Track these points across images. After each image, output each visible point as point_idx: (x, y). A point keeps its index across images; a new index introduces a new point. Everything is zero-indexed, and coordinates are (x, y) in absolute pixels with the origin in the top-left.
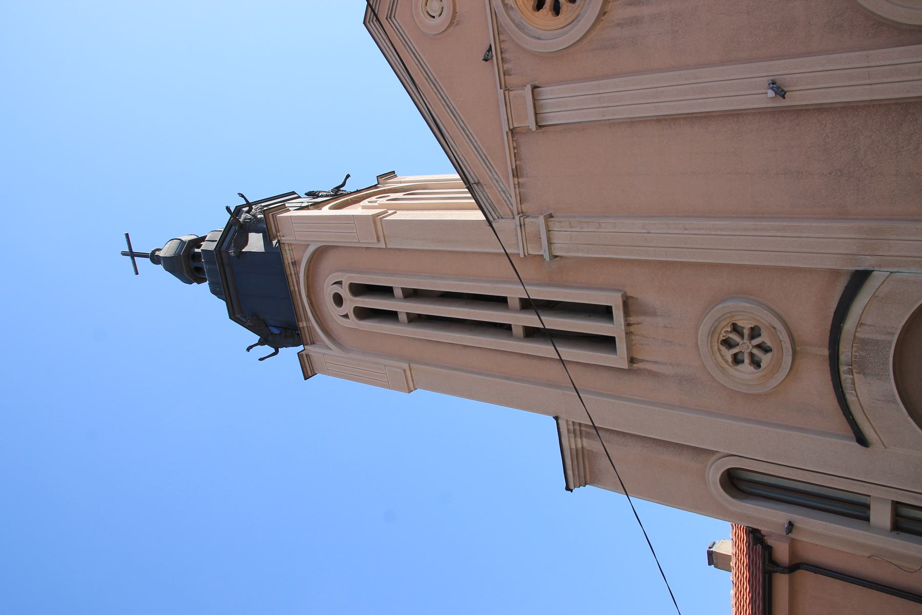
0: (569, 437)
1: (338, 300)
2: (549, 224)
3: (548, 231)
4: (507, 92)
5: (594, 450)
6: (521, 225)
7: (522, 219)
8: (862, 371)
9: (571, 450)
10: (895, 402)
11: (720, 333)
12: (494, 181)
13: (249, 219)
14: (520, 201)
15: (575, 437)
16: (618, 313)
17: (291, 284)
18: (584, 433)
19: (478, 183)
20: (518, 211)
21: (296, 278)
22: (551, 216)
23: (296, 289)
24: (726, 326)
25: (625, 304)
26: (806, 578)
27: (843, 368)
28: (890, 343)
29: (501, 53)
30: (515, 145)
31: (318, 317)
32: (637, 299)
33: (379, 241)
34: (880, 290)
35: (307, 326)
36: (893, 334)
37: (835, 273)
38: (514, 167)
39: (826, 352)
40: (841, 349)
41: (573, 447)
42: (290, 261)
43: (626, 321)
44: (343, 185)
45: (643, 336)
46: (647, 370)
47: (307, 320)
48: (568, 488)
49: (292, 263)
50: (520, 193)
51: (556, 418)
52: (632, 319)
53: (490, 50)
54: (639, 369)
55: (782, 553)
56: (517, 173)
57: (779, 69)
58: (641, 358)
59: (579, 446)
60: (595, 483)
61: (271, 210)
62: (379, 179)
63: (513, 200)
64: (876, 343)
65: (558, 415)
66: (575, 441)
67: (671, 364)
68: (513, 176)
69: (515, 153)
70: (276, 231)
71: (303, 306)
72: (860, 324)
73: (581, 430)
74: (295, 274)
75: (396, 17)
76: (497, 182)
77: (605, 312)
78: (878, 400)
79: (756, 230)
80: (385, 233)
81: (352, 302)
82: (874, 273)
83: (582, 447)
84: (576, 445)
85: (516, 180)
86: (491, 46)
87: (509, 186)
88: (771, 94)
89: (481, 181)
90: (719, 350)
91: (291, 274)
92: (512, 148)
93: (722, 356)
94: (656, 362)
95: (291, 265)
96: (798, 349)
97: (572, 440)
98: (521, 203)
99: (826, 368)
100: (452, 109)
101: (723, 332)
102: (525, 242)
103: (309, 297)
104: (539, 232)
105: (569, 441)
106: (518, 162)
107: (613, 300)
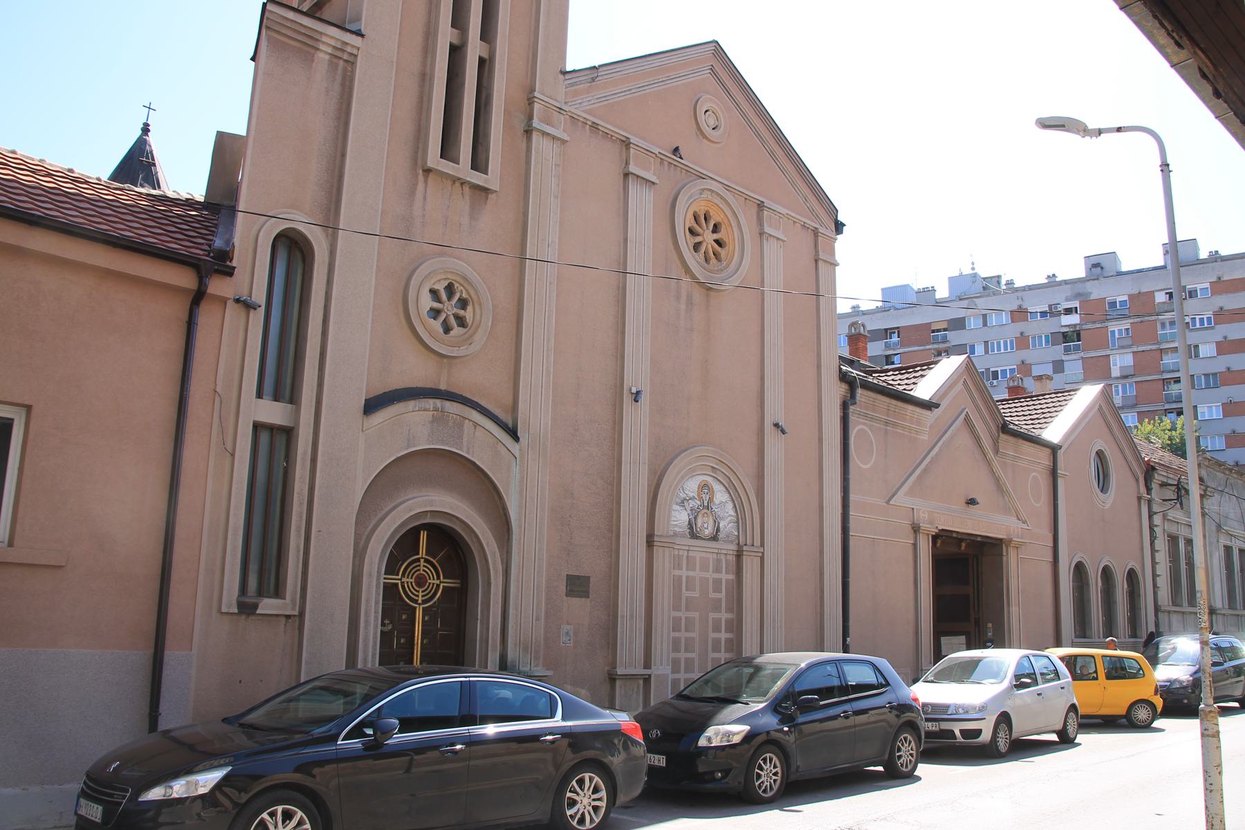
0: (338, 40)
2: (559, 142)
5: (314, 64)
6: (560, 109)
8: (435, 420)
9: (321, 33)
10: (408, 446)
11: (461, 285)
12: (590, 99)
14: (573, 117)
15: (334, 48)
18: (335, 60)
24: (468, 293)
25: (485, 190)
27: (438, 403)
28: (463, 451)
29: (675, 165)
30: (614, 138)
32: (486, 203)
34: (503, 446)
36: (468, 453)
38: (600, 128)
39: (443, 387)
40: (455, 404)
43: (469, 183)
45: (451, 195)
46: (417, 184)
52: (466, 189)
53: (681, 158)
54: (417, 175)
56: (594, 126)
57: (644, 398)
58: (429, 182)
59: (322, 47)
60: (268, 42)
64: (460, 437)
66: (329, 45)
67: (424, 216)
68: (594, 123)
69: (608, 134)
72: (476, 424)
73: (341, 58)
77: (479, 163)
78: (409, 430)
79: (548, 350)
83: (318, 49)
84: (324, 43)
85: (590, 123)
86: (682, 159)
88: (634, 390)
90: (445, 279)
92: (612, 133)
94: (425, 198)
96: (445, 360)
97: (332, 42)
99: (429, 385)
101: (462, 288)
104: (553, 127)
105: (332, 37)
106: (601, 133)
107: (491, 179)
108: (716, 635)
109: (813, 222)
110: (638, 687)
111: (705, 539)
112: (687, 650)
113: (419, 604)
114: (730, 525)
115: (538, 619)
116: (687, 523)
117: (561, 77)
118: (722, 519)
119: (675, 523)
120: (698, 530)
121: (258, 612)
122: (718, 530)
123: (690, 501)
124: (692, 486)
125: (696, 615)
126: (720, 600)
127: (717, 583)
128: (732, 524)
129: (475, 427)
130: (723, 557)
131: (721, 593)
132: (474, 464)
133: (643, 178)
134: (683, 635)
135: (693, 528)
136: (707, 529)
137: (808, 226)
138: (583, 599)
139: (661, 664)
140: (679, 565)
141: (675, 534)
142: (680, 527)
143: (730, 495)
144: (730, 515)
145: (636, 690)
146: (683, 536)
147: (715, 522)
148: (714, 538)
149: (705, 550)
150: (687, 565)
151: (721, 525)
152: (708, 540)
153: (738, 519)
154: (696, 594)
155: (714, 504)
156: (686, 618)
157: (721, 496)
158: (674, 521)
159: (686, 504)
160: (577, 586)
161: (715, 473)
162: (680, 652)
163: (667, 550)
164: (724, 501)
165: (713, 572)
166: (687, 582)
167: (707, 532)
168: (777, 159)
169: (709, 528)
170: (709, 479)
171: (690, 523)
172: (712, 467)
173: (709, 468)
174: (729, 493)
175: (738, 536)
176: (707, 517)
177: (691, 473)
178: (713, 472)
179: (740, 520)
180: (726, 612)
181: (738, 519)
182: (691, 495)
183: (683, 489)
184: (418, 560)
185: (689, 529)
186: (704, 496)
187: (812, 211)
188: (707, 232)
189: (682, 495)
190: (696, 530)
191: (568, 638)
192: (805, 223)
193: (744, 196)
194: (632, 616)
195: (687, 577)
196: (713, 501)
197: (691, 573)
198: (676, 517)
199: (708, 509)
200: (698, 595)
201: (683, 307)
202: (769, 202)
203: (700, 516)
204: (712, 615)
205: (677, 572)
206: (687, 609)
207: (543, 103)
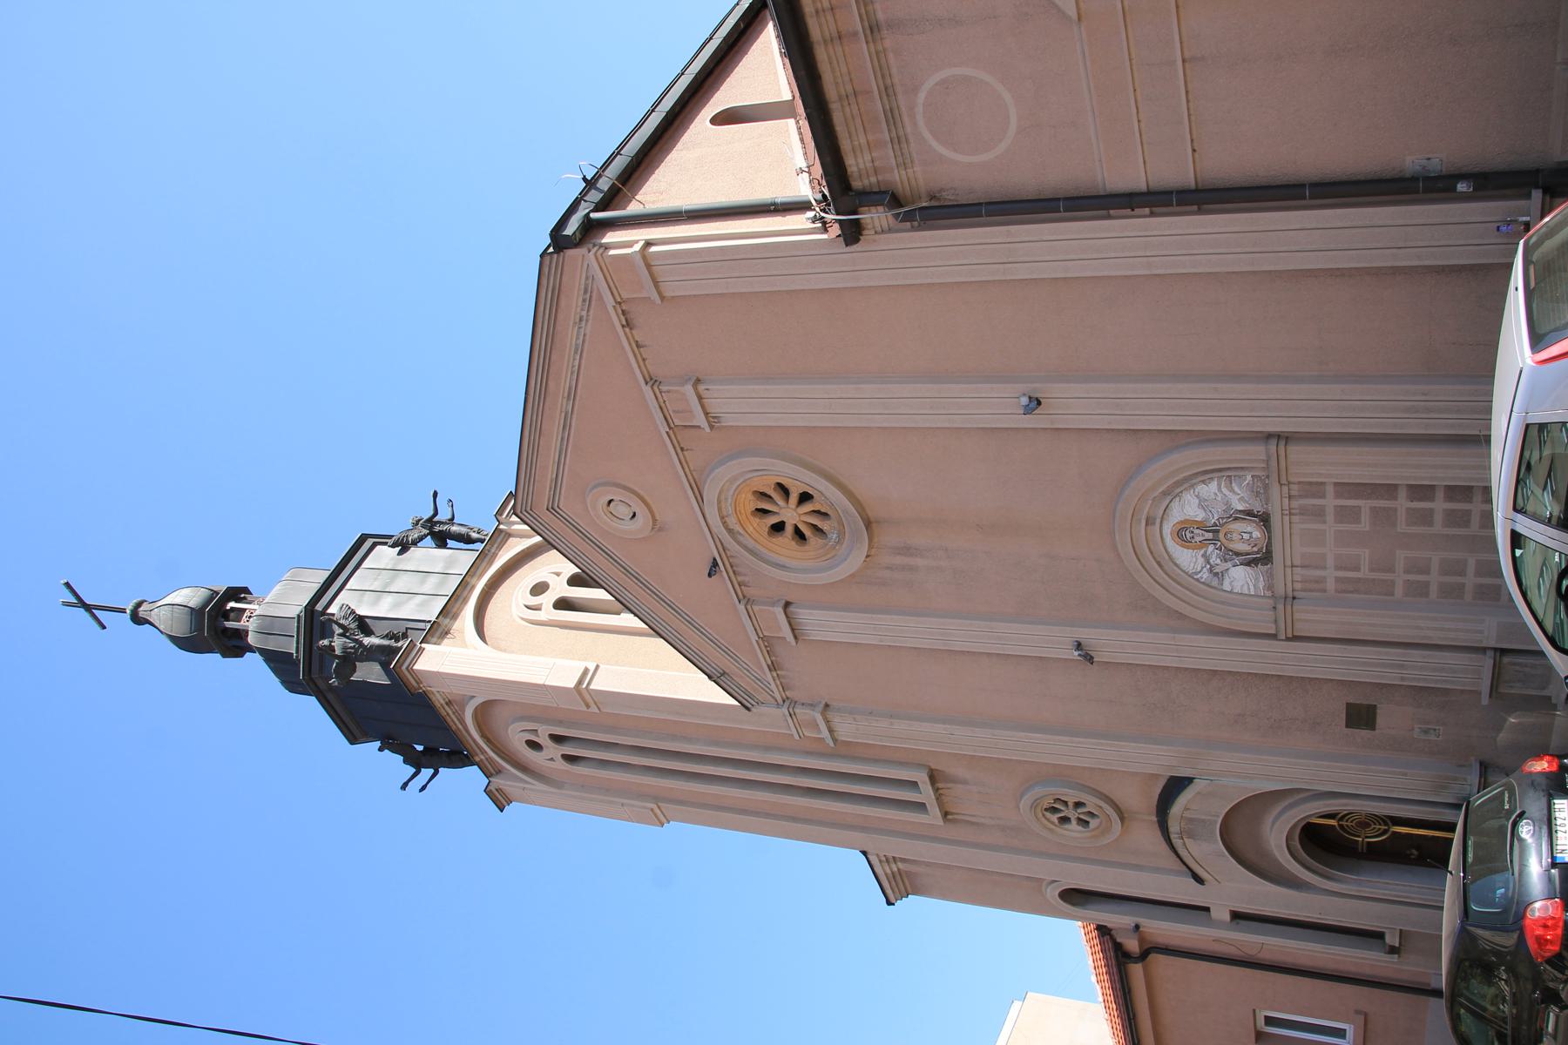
1: (534, 745)
3: (700, 398)
4: (749, 607)
6: (790, 715)
7: (655, 388)
9: (886, 874)
12: (745, 671)
13: (351, 648)
16: (926, 794)
17: (451, 724)
19: (724, 673)
20: (782, 698)
21: (456, 716)
22: (698, 381)
23: (460, 727)
26: (1159, 961)
28: (1216, 822)
29: (732, 566)
31: (504, 753)
32: (942, 771)
33: (588, 706)
35: (487, 759)
36: (1218, 816)
37: (1156, 776)
38: (770, 663)
41: (889, 871)
42: (442, 702)
44: (436, 513)
47: (483, 752)
48: (889, 903)
49: (447, 704)
50: (781, 683)
51: (864, 853)
55: (1132, 945)
56: (773, 667)
59: (895, 869)
61: (401, 661)
62: (499, 518)
63: (773, 686)
65: (865, 849)
68: (770, 670)
69: (768, 651)
70: (418, 683)
71: (474, 741)
74: (454, 713)
75: (561, 507)
76: (748, 671)
80: (596, 700)
81: (553, 751)
82: (1195, 780)
86: (715, 559)
87: (764, 673)
89: (727, 671)
90: (1044, 815)
91: (448, 714)
92: (763, 648)
93: (1048, 820)
95: (445, 706)
98: (784, 691)
100: (669, 603)
102: (797, 725)
103: (483, 736)
108: (1438, 518)
109: (600, 297)
110: (1514, 664)
111: (1270, 538)
112: (1462, 573)
113: (1389, 828)
114: (1236, 489)
115: (1405, 774)
116: (1245, 567)
117: (753, 709)
118: (1228, 504)
119: (1252, 588)
120: (1255, 549)
121: (1397, 945)
122: (1249, 513)
124: (1188, 559)
125: (1401, 556)
126: (1374, 510)
127: (1344, 514)
128: (1233, 485)
129: (1188, 809)
130: (1295, 504)
131: (1360, 507)
132: (1227, 812)
133: (790, 624)
134: (1434, 579)
135: (1254, 559)
137: (623, 318)
138: (1378, 711)
139: (1481, 632)
140: (1317, 582)
141: (1270, 587)
142: (1257, 579)
144: (1219, 489)
145: (1517, 668)
146: (1270, 576)
147: (1236, 519)
148: (1264, 520)
150: (1317, 568)
152: (1269, 532)
154: (1365, 554)
156: (1407, 571)
157: (1188, 508)
158: (1249, 589)
159: (1217, 570)
160: (1361, 716)
161: (1155, 519)
162: (1463, 585)
163: (1297, 616)
164: (1197, 501)
165: (1325, 522)
166: (1346, 569)
167: (1257, 534)
168: (570, 388)
169: (1249, 529)
170: (1168, 529)
171: (1248, 564)
172: (1147, 525)
173: (1149, 528)
176: (1231, 533)
177: (1165, 563)
178: (1154, 524)
179: (1226, 473)
180: (1395, 498)
182: (1201, 561)
183: (1197, 573)
184: (1339, 825)
187: (588, 302)
188: (783, 511)
189: (1205, 575)
190: (1257, 553)
191: (1432, 731)
192: (623, 326)
193: (682, 457)
194: (1401, 667)
195: (1338, 568)
196: (1201, 522)
197: (1330, 562)
198: (1243, 586)
199: (1218, 531)
200: (1367, 551)
201: (919, 562)
202: (662, 429)
203: (1233, 546)
204: (1402, 527)
205: (1331, 585)
206: (1391, 570)
207: (800, 731)
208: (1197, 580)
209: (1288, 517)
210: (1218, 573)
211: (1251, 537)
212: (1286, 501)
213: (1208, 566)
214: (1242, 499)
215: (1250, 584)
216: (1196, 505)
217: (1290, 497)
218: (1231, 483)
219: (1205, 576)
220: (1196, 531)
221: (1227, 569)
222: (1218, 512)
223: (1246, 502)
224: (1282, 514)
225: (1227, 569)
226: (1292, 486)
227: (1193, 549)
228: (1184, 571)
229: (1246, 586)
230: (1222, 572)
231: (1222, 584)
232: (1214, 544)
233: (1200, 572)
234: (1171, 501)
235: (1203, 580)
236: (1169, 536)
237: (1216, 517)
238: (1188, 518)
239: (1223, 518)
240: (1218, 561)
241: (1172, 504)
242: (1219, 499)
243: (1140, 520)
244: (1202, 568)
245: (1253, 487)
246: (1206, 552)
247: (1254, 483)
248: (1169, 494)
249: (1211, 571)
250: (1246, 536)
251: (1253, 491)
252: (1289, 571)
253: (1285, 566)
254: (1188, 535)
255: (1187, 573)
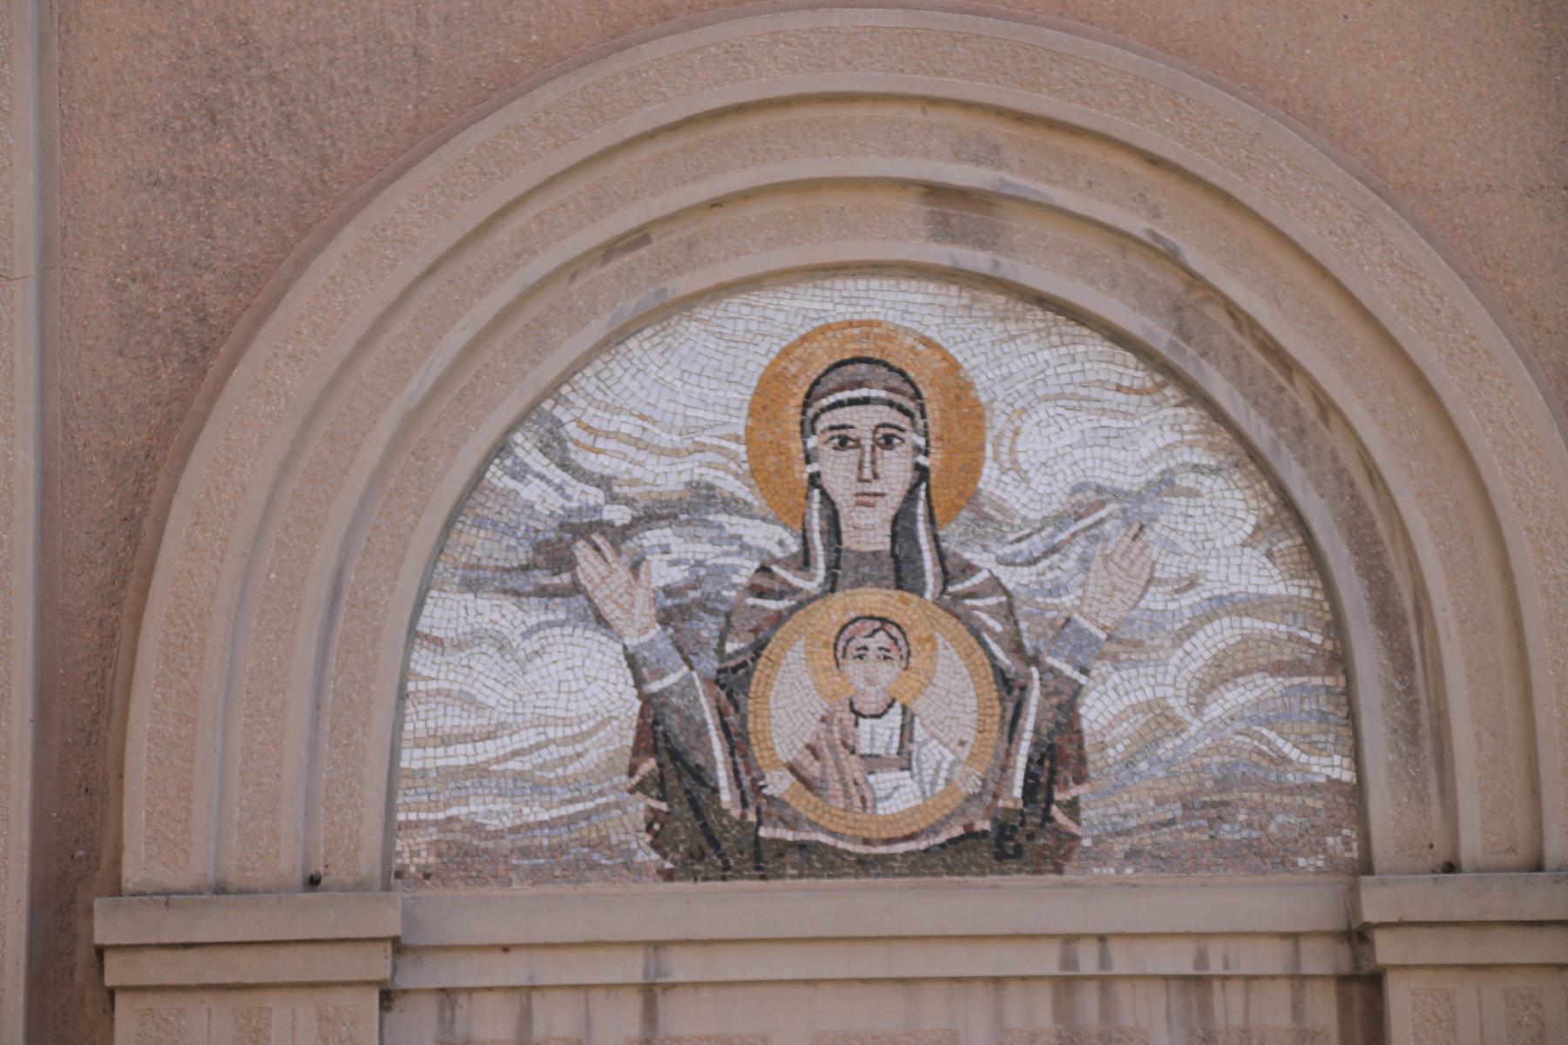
111: (864, 865)
114: (1235, 697)
119: (460, 755)
120: (779, 784)
123: (652, 537)
135: (701, 776)
136: (905, 760)
142: (532, 785)
143: (1217, 414)
147: (1008, 685)
149: (874, 963)
151: (1095, 712)
152: (920, 864)
153: (1336, 627)
155: (987, 522)
164: (1123, 482)
169: (933, 754)
172: (935, 192)
173: (910, 206)
174: (1195, 395)
175: (1357, 792)
178: (943, 231)
181: (1336, 627)
183: (554, 445)
185: (657, 786)
186: (838, 472)
190: (750, 791)
196: (969, 496)
198: (469, 702)
208: (501, 448)
209: (1054, 970)
210: (570, 564)
211: (873, 762)
212: (1180, 960)
213: (618, 515)
214: (1162, 720)
215: (507, 744)
216: (1104, 476)
217: (1198, 983)
218: (1277, 669)
219: (531, 491)
220: (896, 470)
221: (601, 621)
222: (1056, 590)
223: (1145, 744)
224: (1069, 939)
225: (601, 621)
226: (1282, 994)
227: (750, 438)
228: (566, 377)
229: (471, 722)
230: (576, 588)
231: (472, 585)
232: (804, 561)
233: (565, 465)
234: (1118, 337)
235: (497, 476)
236: (843, 312)
237: (1009, 578)
238: (997, 422)
239: (1008, 612)
240: (662, 573)
241: (1097, 346)
242: (1156, 599)
243: (992, 155)
244: (604, 482)
245: (1263, 785)
246: (730, 505)
247: (1292, 790)
248: (1183, 332)
249: (583, 528)
250: (879, 735)
251: (1223, 783)
252: (631, 968)
253: (657, 946)
254: (864, 421)
255: (553, 391)
